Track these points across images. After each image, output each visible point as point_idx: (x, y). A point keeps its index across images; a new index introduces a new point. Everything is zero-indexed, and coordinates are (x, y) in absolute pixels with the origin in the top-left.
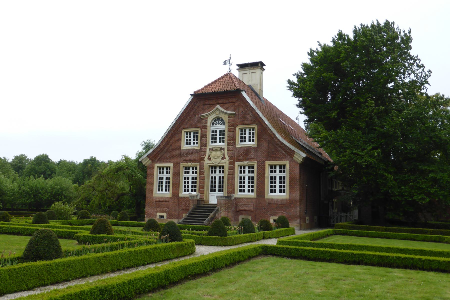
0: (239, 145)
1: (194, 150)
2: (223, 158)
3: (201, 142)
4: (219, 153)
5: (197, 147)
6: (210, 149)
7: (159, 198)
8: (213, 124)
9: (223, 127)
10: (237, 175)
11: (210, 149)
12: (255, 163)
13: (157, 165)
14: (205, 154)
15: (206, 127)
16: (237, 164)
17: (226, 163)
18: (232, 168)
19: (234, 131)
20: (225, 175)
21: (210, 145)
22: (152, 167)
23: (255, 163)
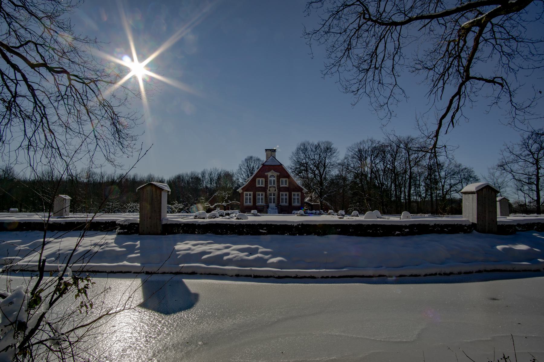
0: (281, 186)
1: (261, 187)
2: (275, 191)
3: (265, 183)
4: (274, 189)
5: (263, 186)
6: (270, 187)
7: (247, 206)
8: (270, 177)
9: (274, 179)
10: (281, 197)
11: (270, 187)
12: (287, 193)
13: (245, 193)
14: (267, 189)
15: (267, 178)
16: (281, 193)
17: (276, 192)
18: (279, 194)
19: (279, 180)
20: (276, 197)
21: (269, 186)
22: (243, 193)
23: (287, 193)
